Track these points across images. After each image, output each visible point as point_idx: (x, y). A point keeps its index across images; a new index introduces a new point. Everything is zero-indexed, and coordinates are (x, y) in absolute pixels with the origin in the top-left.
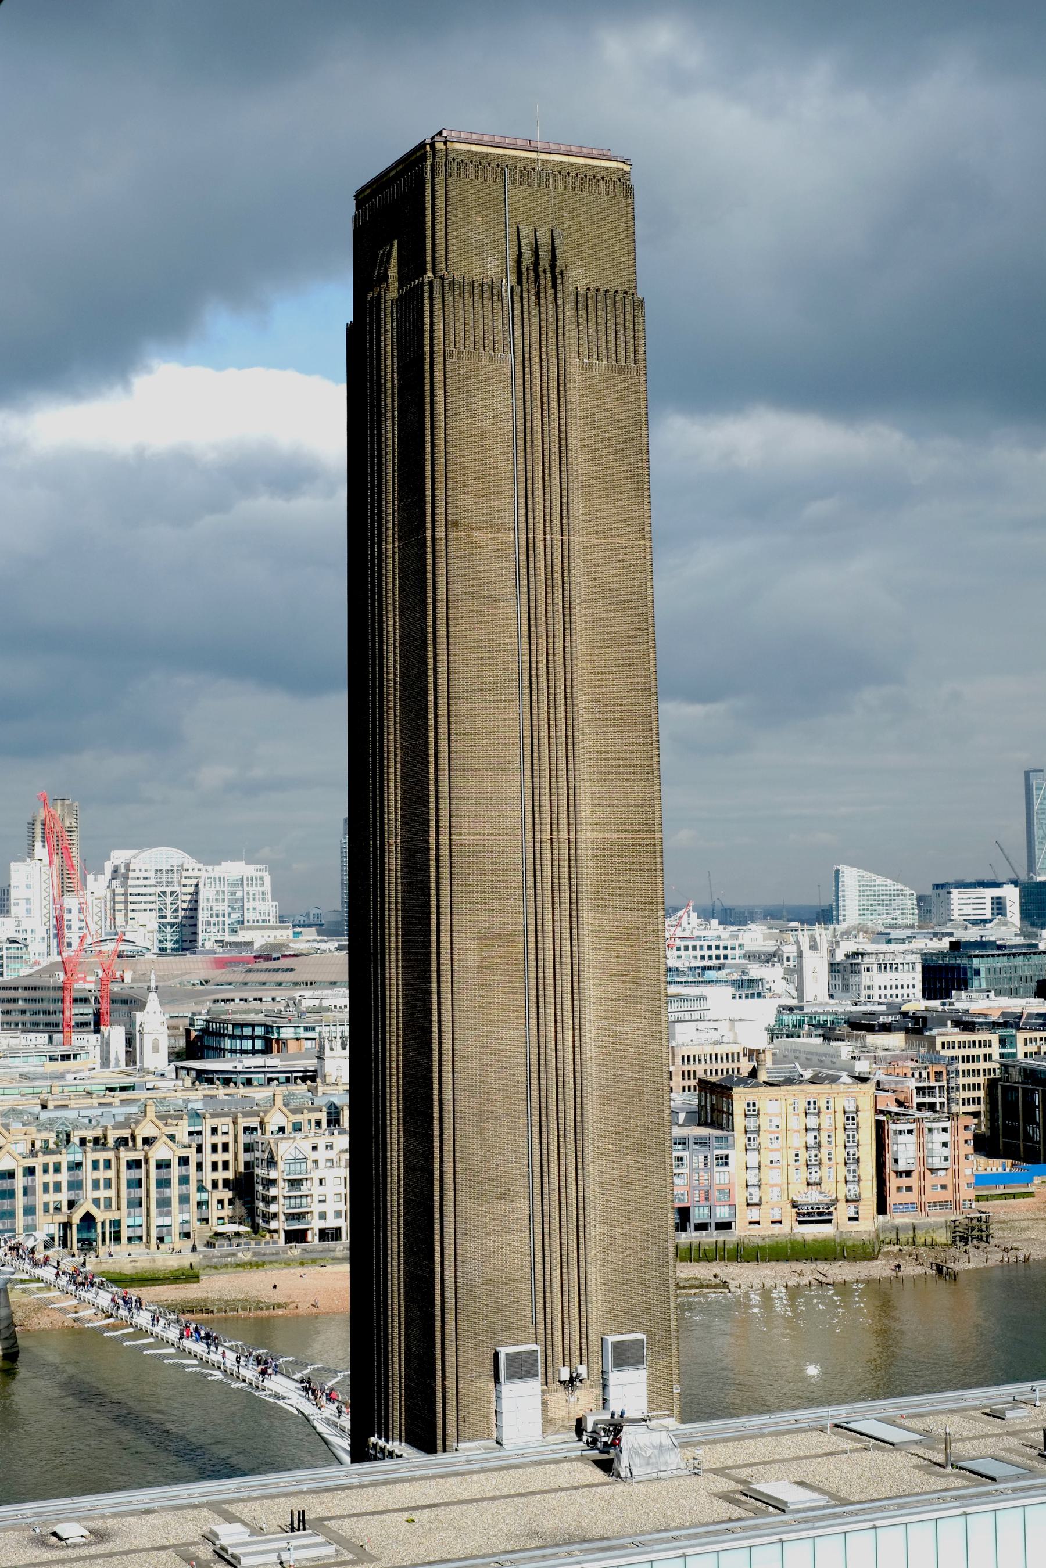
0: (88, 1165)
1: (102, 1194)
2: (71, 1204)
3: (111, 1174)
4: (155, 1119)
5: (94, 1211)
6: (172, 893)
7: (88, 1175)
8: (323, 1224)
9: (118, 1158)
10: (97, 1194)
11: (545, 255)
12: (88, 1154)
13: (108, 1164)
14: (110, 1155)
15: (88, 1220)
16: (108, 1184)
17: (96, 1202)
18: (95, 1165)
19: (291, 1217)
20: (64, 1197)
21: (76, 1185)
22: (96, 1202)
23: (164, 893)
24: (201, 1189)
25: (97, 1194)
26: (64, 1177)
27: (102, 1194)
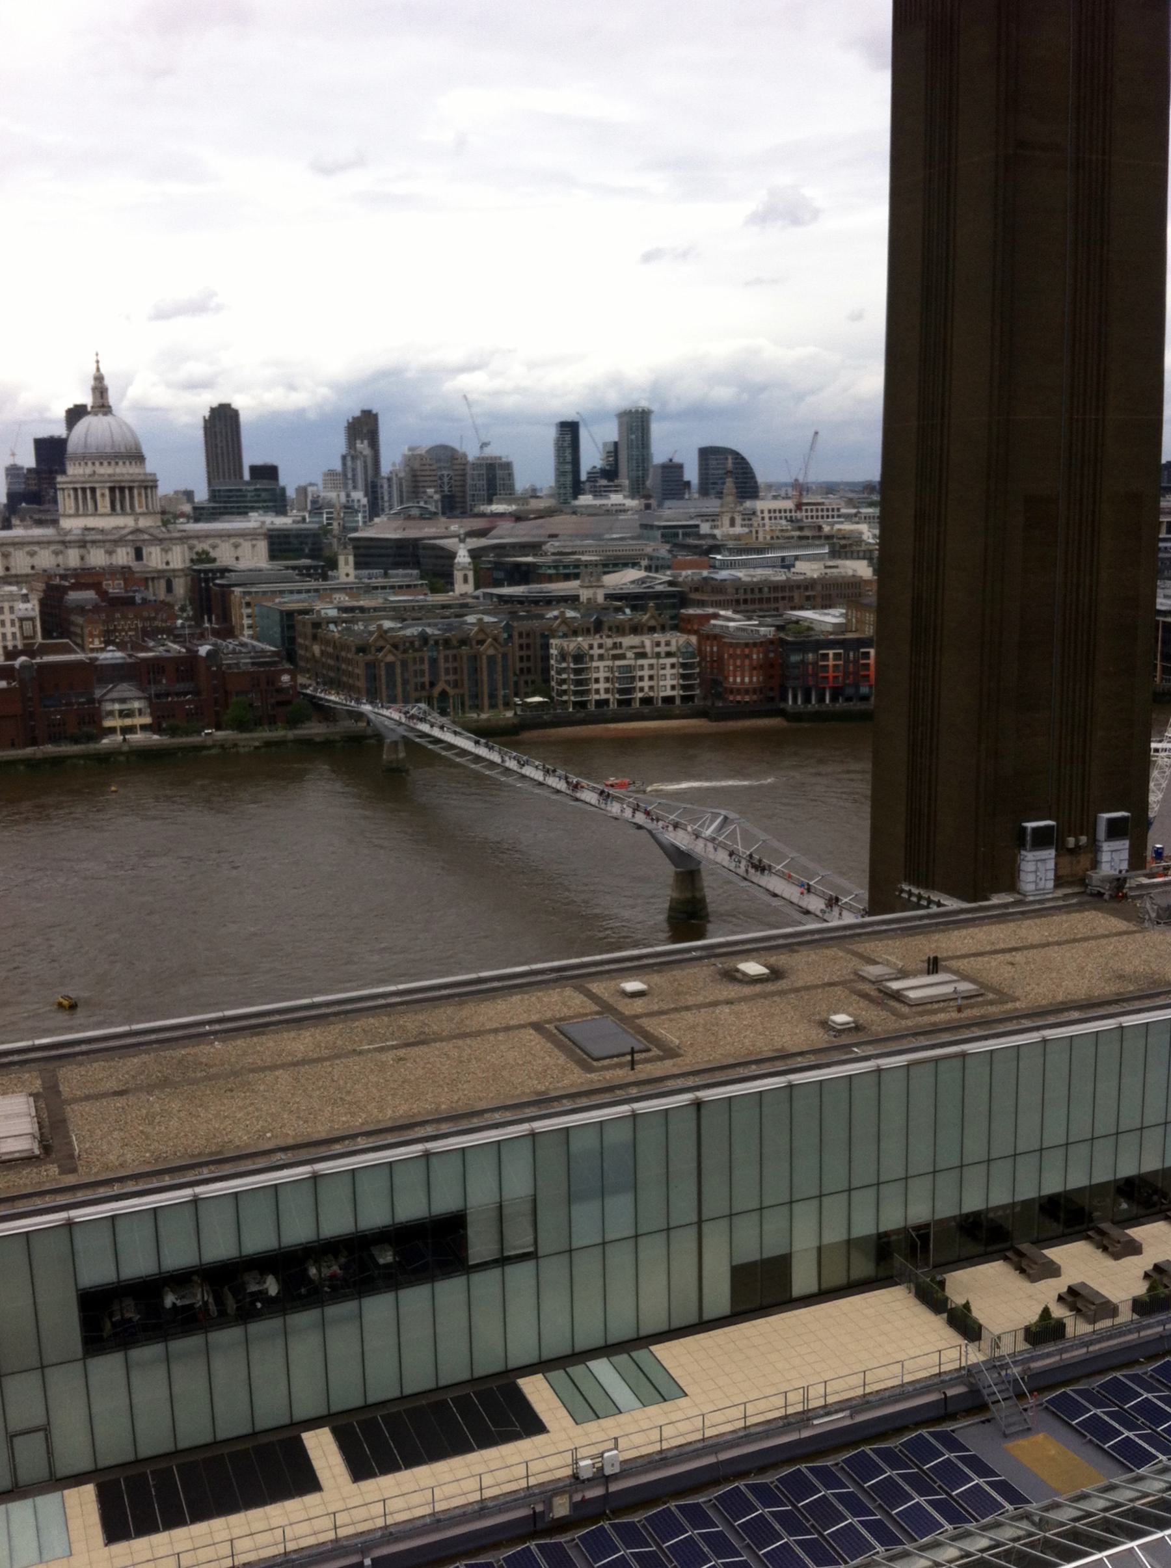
1: (451, 677)
2: (432, 684)
5: (448, 689)
6: (448, 475)
8: (597, 697)
10: (448, 678)
15: (444, 695)
17: (448, 682)
18: (446, 659)
19: (576, 693)
20: (426, 679)
22: (448, 682)
23: (443, 475)
24: (515, 674)
25: (448, 678)
26: (426, 666)
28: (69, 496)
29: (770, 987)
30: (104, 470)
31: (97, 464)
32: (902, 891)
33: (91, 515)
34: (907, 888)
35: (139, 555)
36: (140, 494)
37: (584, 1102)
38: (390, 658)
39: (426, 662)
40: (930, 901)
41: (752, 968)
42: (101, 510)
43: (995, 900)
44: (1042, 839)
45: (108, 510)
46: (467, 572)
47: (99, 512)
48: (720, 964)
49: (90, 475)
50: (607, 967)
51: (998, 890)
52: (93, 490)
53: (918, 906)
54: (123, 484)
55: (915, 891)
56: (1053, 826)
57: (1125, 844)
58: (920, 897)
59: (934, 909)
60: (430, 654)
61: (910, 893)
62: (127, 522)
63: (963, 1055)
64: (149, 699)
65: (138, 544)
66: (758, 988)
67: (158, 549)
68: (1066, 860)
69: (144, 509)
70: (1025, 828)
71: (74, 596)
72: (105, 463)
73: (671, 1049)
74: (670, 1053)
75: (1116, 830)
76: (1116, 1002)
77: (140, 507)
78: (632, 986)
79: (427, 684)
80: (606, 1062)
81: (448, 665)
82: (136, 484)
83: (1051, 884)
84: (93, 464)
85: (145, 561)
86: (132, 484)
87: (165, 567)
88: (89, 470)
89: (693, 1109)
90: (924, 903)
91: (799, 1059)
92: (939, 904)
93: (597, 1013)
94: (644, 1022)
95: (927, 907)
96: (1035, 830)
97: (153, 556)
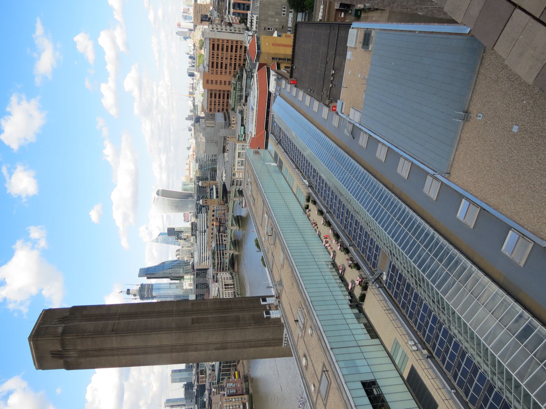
11: (59, 320)
29: (308, 358)
32: (285, 346)
34: (283, 345)
37: (337, 376)
40: (286, 338)
41: (304, 362)
43: (282, 321)
44: (268, 313)
48: (304, 369)
50: (311, 402)
51: (281, 322)
53: (287, 341)
55: (284, 342)
56: (265, 312)
57: (267, 299)
58: (285, 340)
59: (287, 336)
61: (285, 343)
63: (311, 301)
66: (309, 359)
68: (272, 308)
70: (266, 317)
73: (323, 366)
74: (324, 365)
75: (264, 300)
76: (297, 282)
78: (313, 388)
80: (329, 379)
83: (278, 311)
89: (333, 349)
90: (286, 339)
91: (319, 334)
92: (286, 335)
93: (320, 393)
94: (319, 378)
95: (287, 338)
96: (266, 315)
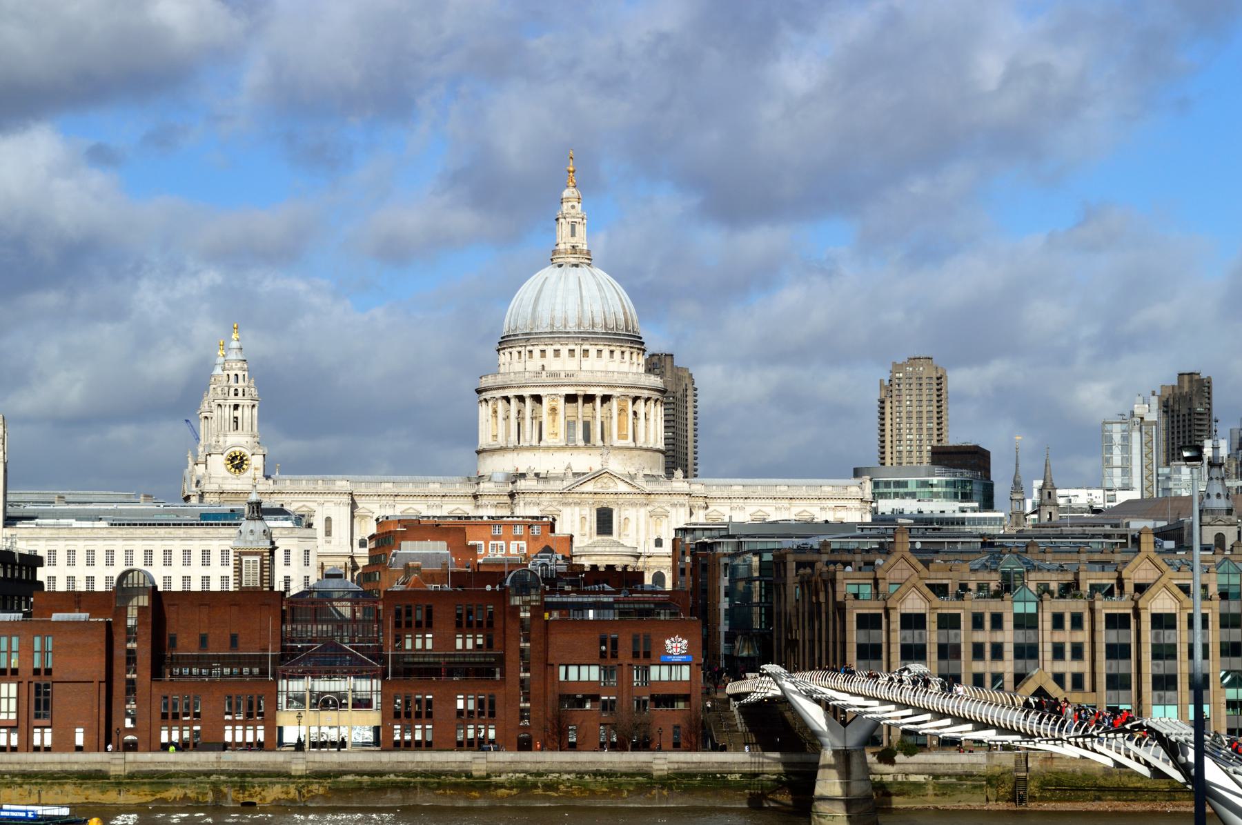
0: (1046, 622)
1: (1068, 667)
2: (1019, 678)
3: (1083, 636)
4: (1152, 555)
5: (1053, 689)
7: (1047, 637)
9: (1092, 611)
10: (1060, 667)
12: (1046, 604)
13: (1077, 622)
14: (1080, 606)
16: (1077, 652)
17: (1059, 679)
18: (1058, 622)
20: (1007, 667)
21: (1026, 652)
22: (1059, 679)
25: (1060, 667)
26: (1008, 637)
27: (1068, 667)
28: (495, 412)
30: (564, 364)
31: (550, 351)
33: (531, 448)
35: (605, 522)
36: (622, 410)
38: (914, 604)
39: (1008, 623)
42: (547, 440)
45: (560, 440)
46: (1223, 530)
47: (542, 444)
49: (538, 374)
52: (537, 399)
54: (590, 391)
60: (1019, 608)
62: (585, 461)
64: (383, 677)
65: (606, 501)
67: (643, 511)
69: (629, 442)
71: (409, 548)
72: (564, 351)
77: (622, 436)
79: (1009, 678)
81: (1059, 637)
82: (615, 392)
84: (543, 351)
85: (615, 537)
86: (607, 392)
87: (653, 549)
88: (535, 363)
97: (632, 526)
